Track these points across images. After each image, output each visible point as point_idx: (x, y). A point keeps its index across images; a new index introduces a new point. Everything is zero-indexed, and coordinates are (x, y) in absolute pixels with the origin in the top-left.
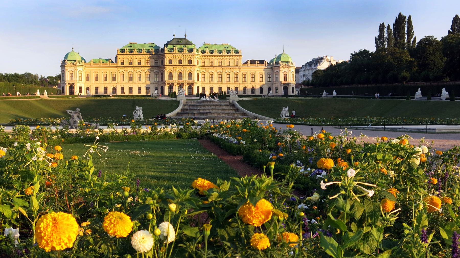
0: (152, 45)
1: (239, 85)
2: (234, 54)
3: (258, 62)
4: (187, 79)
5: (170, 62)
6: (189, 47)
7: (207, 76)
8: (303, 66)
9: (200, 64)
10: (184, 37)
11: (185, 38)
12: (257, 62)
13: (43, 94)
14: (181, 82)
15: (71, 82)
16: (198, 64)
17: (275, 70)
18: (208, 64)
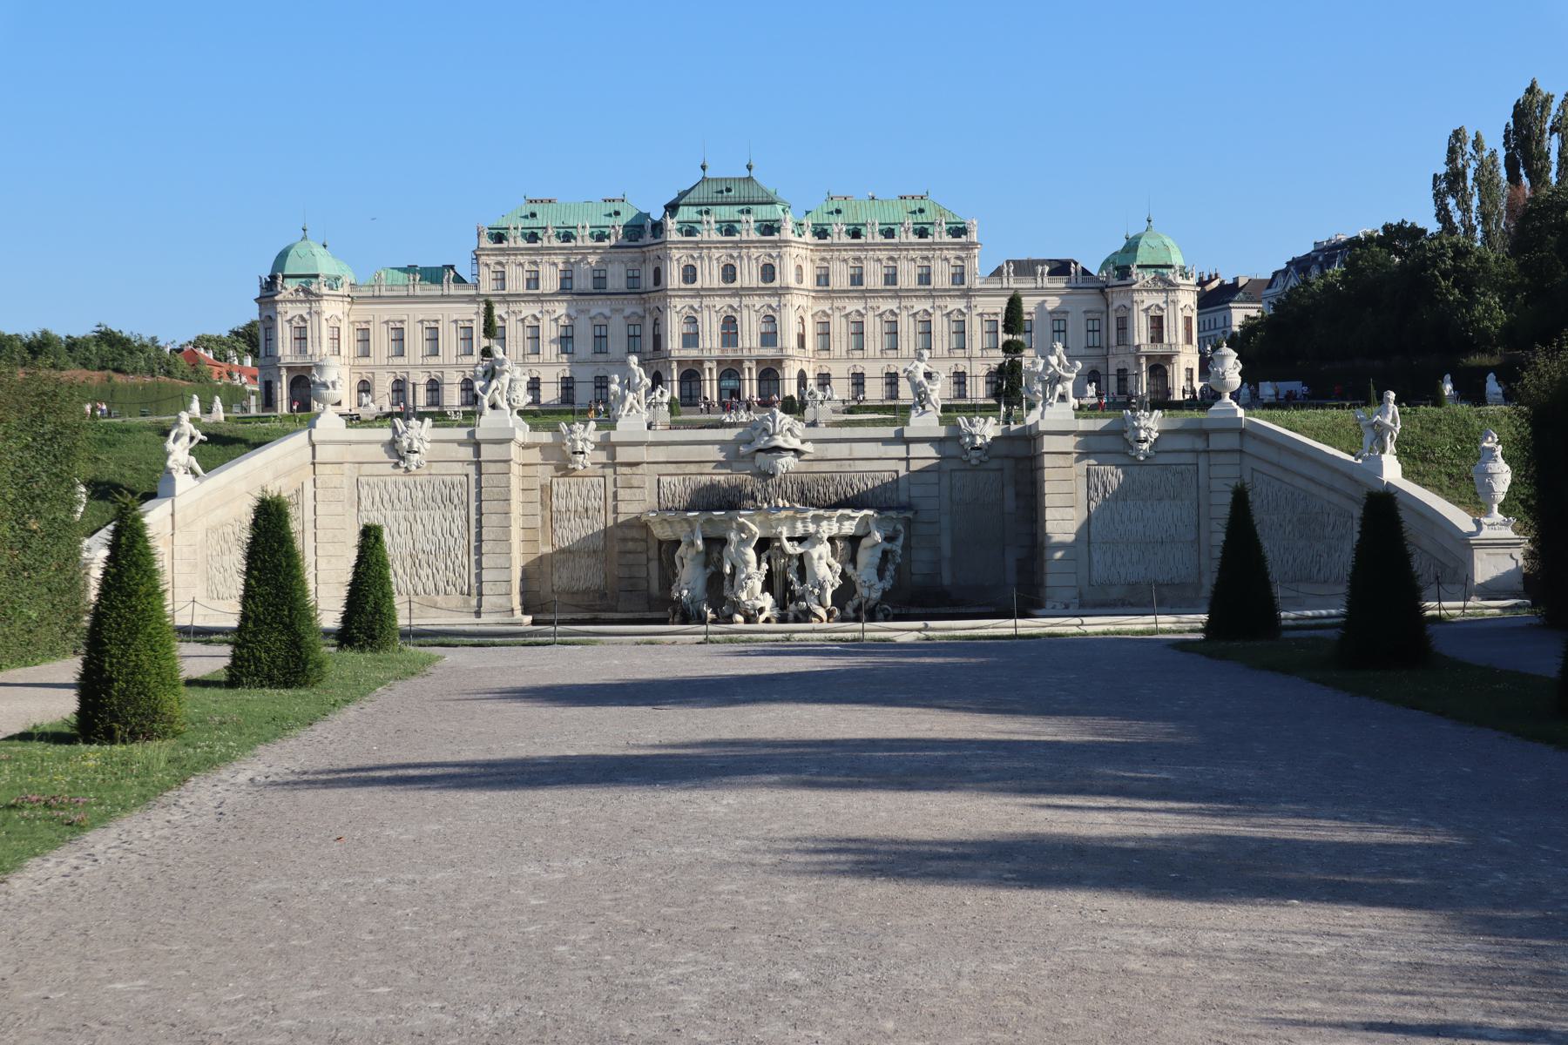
0: (617, 206)
1: (967, 363)
3: (1047, 269)
4: (756, 341)
5: (690, 274)
6: (764, 212)
7: (839, 328)
8: (1275, 274)
9: (809, 281)
10: (746, 174)
11: (750, 179)
12: (1040, 269)
13: (209, 411)
14: (730, 354)
15: (299, 361)
16: (800, 280)
17: (1117, 300)
18: (840, 280)
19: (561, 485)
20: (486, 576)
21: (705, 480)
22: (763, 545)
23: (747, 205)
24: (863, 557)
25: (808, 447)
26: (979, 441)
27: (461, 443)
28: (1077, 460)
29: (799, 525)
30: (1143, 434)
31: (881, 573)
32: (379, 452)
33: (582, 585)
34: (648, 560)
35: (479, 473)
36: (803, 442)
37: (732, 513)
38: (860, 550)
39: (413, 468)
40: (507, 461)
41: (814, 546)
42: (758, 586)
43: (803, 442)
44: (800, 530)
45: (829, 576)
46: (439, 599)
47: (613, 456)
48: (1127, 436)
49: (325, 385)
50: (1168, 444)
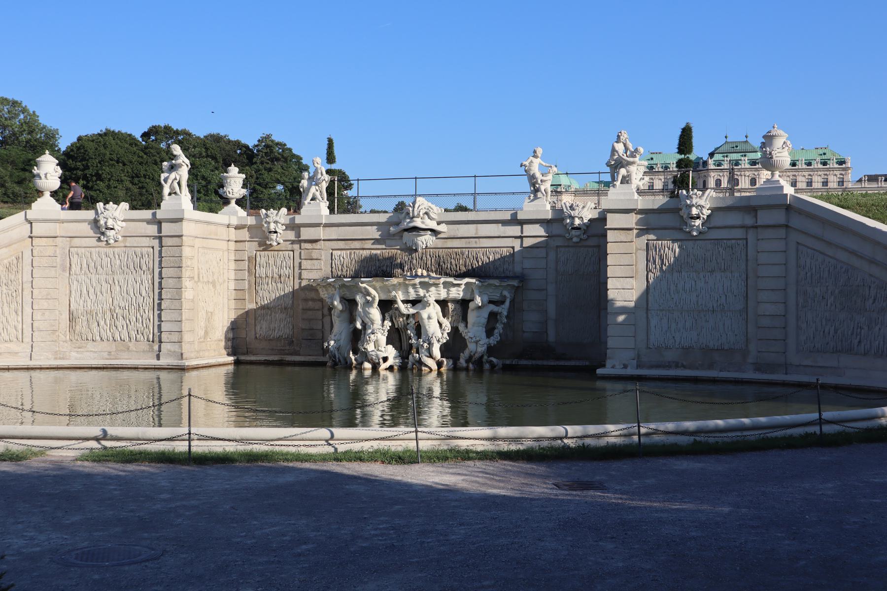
2: (836, 166)
10: (745, 139)
11: (746, 142)
19: (263, 257)
20: (164, 327)
21: (366, 253)
22: (386, 306)
23: (744, 153)
24: (472, 317)
25: (443, 228)
26: (577, 222)
27: (149, 222)
28: (638, 236)
29: (411, 290)
30: (694, 211)
31: (489, 333)
32: (86, 229)
33: (276, 334)
34: (323, 316)
35: (161, 246)
36: (439, 223)
37: (357, 279)
38: (469, 311)
39: (112, 241)
40: (182, 236)
41: (424, 308)
42: (383, 339)
43: (439, 223)
44: (412, 296)
45: (439, 334)
46: (130, 344)
47: (298, 235)
48: (682, 213)
49: (38, 176)
50: (718, 221)
